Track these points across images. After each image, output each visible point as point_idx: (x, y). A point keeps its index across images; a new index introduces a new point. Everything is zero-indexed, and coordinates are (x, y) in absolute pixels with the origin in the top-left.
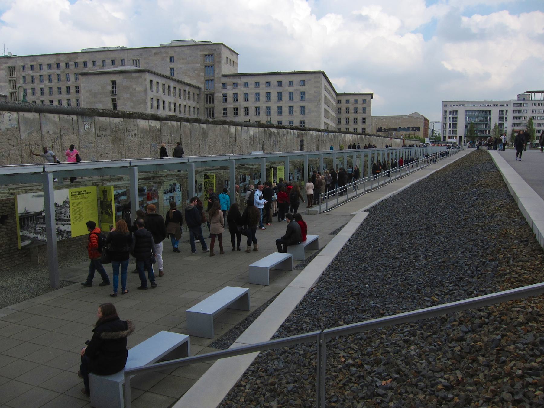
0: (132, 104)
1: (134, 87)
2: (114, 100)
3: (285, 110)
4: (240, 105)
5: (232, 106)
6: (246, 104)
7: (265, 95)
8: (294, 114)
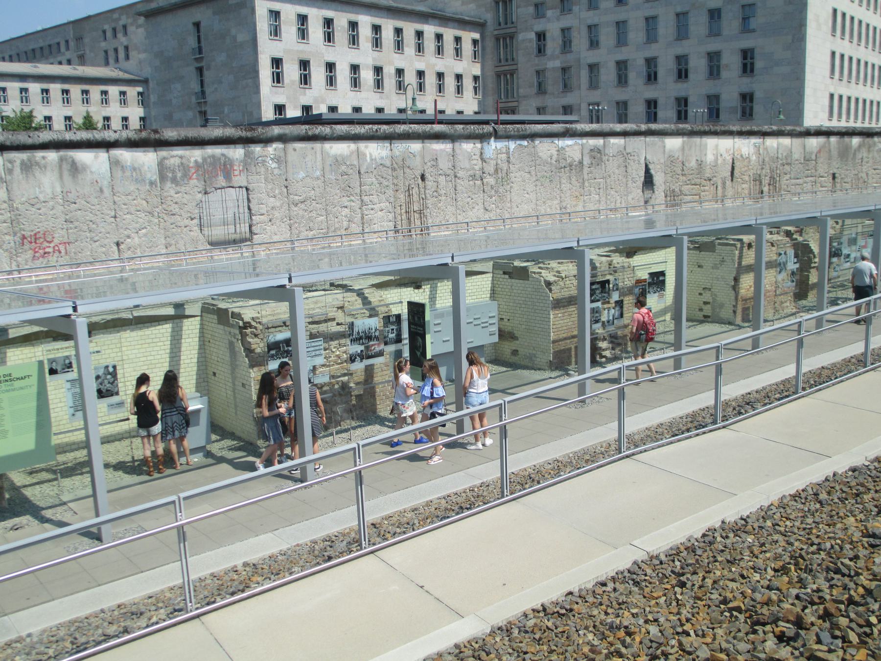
0: (231, 77)
1: (233, 32)
2: (200, 70)
3: (698, 65)
4: (579, 60)
5: (557, 64)
6: (591, 57)
7: (642, 24)
8: (724, 74)
